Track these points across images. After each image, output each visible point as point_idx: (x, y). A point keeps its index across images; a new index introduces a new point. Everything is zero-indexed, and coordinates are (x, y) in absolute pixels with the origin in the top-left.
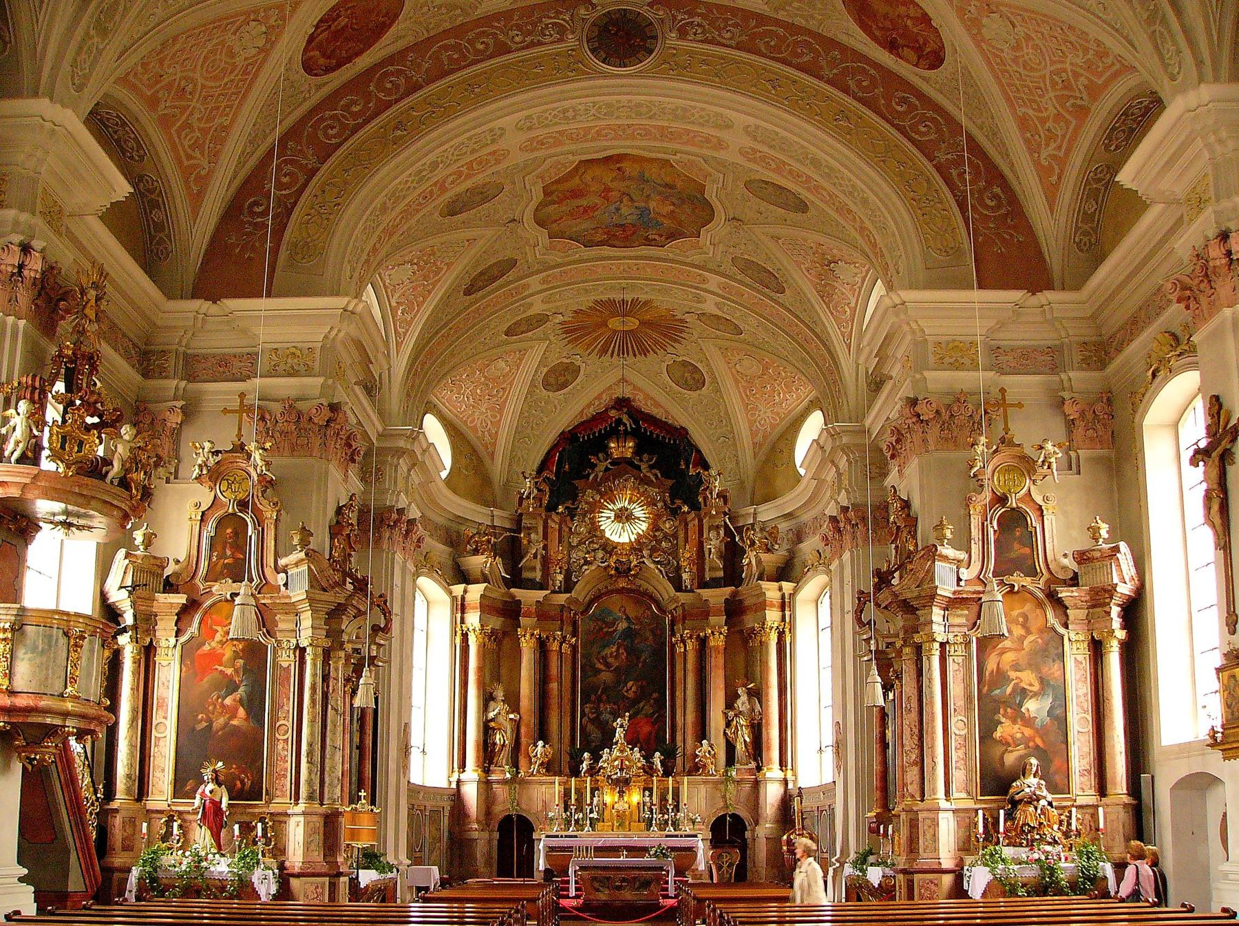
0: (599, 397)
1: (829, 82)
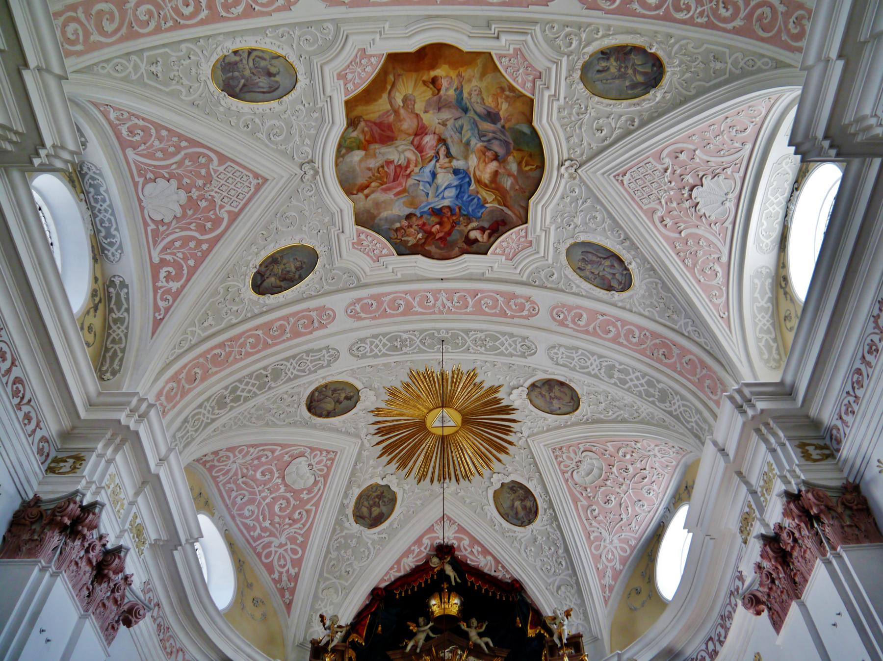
0: (418, 542)
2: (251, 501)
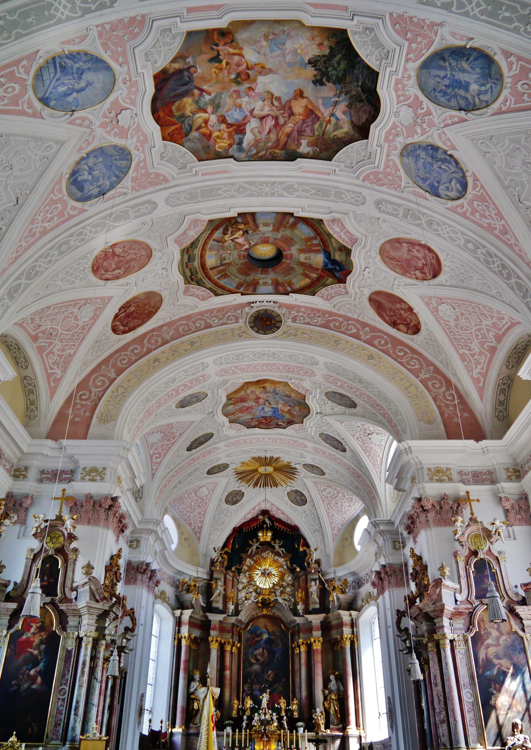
0: (254, 509)
1: (365, 342)
2: (183, 504)
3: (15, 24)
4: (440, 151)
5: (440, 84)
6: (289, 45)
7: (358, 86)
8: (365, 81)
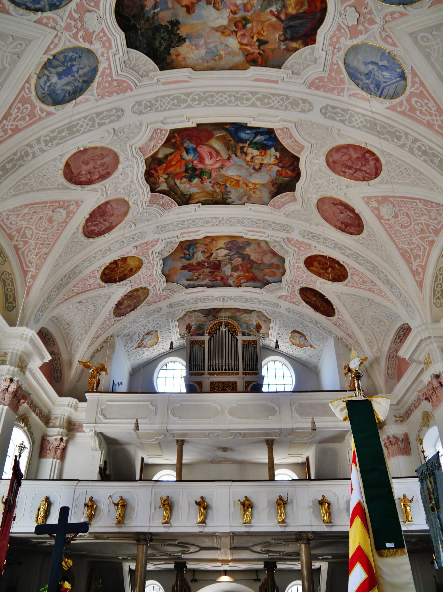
3: (389, 133)
4: (47, 7)
5: (78, 64)
6: (203, 52)
7: (141, 29)
8: (136, 36)
